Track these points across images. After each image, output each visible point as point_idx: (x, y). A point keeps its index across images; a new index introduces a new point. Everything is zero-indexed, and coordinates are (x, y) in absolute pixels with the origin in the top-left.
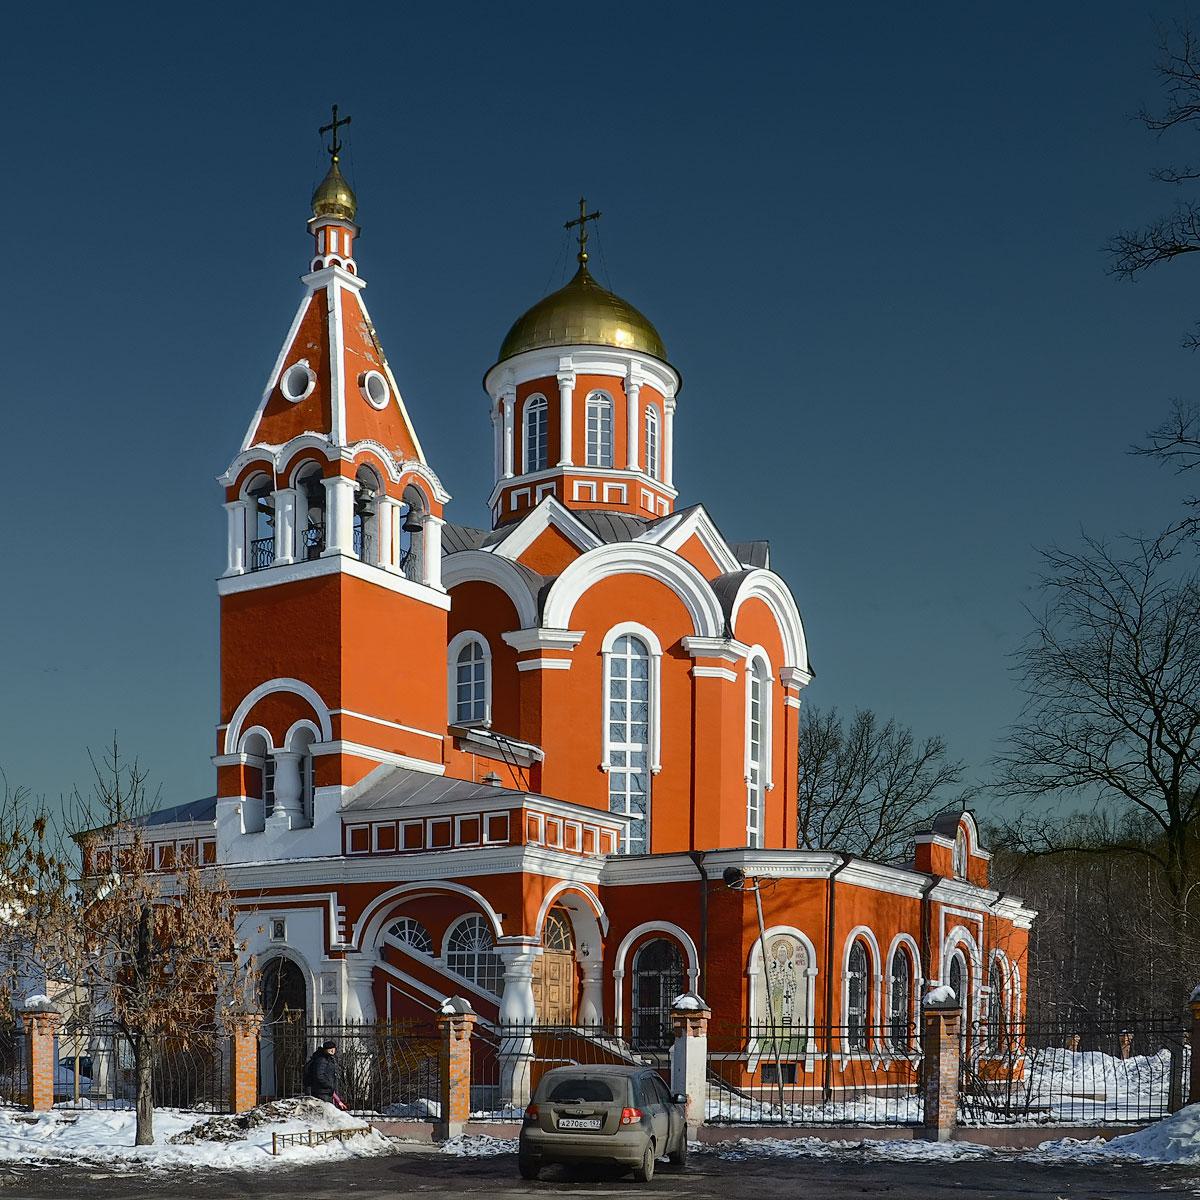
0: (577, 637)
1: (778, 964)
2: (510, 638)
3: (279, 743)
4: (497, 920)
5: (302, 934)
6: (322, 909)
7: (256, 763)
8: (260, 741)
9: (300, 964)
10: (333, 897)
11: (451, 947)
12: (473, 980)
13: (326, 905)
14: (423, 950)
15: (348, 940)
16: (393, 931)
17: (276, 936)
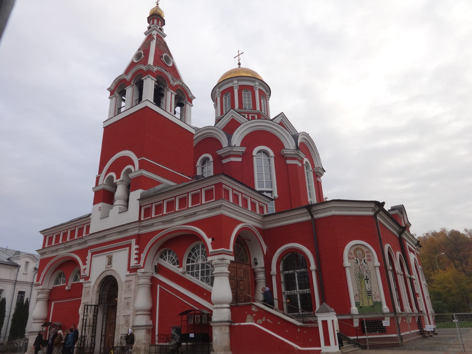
0: (243, 149)
1: (359, 261)
2: (220, 152)
3: (118, 177)
4: (209, 241)
5: (120, 263)
6: (128, 248)
7: (108, 187)
8: (111, 178)
9: (117, 278)
10: (133, 241)
11: (188, 261)
12: (198, 278)
13: (130, 245)
14: (174, 264)
15: (139, 263)
16: (161, 257)
17: (108, 265)
